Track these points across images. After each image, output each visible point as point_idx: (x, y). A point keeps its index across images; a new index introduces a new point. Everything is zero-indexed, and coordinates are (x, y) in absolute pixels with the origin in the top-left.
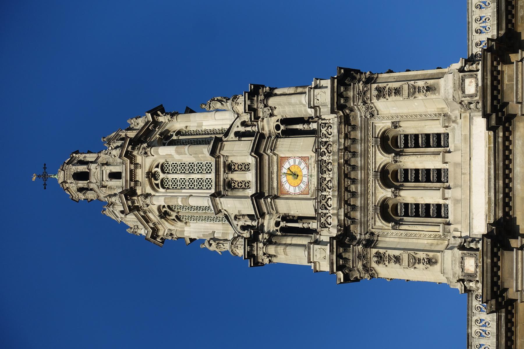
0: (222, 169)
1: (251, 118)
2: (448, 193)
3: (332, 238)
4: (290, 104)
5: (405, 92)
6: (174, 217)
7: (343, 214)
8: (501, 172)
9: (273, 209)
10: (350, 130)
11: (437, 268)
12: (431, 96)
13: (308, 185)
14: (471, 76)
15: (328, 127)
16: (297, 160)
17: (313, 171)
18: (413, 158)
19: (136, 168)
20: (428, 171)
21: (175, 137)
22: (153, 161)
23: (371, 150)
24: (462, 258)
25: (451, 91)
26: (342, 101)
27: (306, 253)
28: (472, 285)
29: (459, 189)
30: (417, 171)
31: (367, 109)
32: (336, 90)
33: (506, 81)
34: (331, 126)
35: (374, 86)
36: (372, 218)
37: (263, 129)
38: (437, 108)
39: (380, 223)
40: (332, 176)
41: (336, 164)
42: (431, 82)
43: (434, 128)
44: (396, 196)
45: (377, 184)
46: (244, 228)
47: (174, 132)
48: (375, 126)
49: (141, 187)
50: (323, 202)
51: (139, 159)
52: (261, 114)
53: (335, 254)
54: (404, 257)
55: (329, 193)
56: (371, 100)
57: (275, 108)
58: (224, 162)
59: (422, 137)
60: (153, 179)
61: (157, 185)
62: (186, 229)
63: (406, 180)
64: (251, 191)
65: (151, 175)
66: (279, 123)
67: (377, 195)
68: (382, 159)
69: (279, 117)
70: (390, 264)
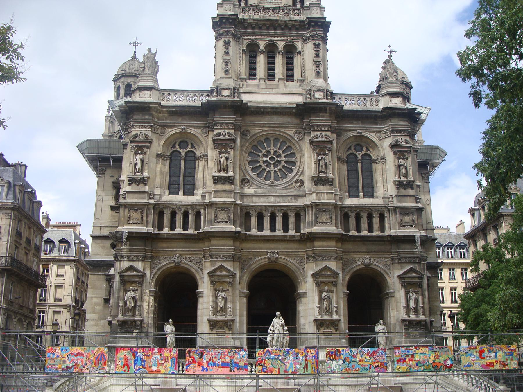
3: (237, 15)
5: (317, 60)
8: (274, 110)
11: (224, 75)
12: (314, 73)
18: (281, 62)
20: (274, 70)
23: (285, 39)
24: (229, 89)
25: (317, 85)
26: (313, 24)
28: (215, 94)
29: (265, 87)
30: (274, 64)
31: (308, 38)
33: (321, 114)
35: (321, 42)
39: (246, 42)
40: (271, 16)
41: (278, 19)
42: (322, 74)
43: (297, 75)
44: (260, 52)
50: (256, 10)
63: (269, 57)
68: (281, 45)
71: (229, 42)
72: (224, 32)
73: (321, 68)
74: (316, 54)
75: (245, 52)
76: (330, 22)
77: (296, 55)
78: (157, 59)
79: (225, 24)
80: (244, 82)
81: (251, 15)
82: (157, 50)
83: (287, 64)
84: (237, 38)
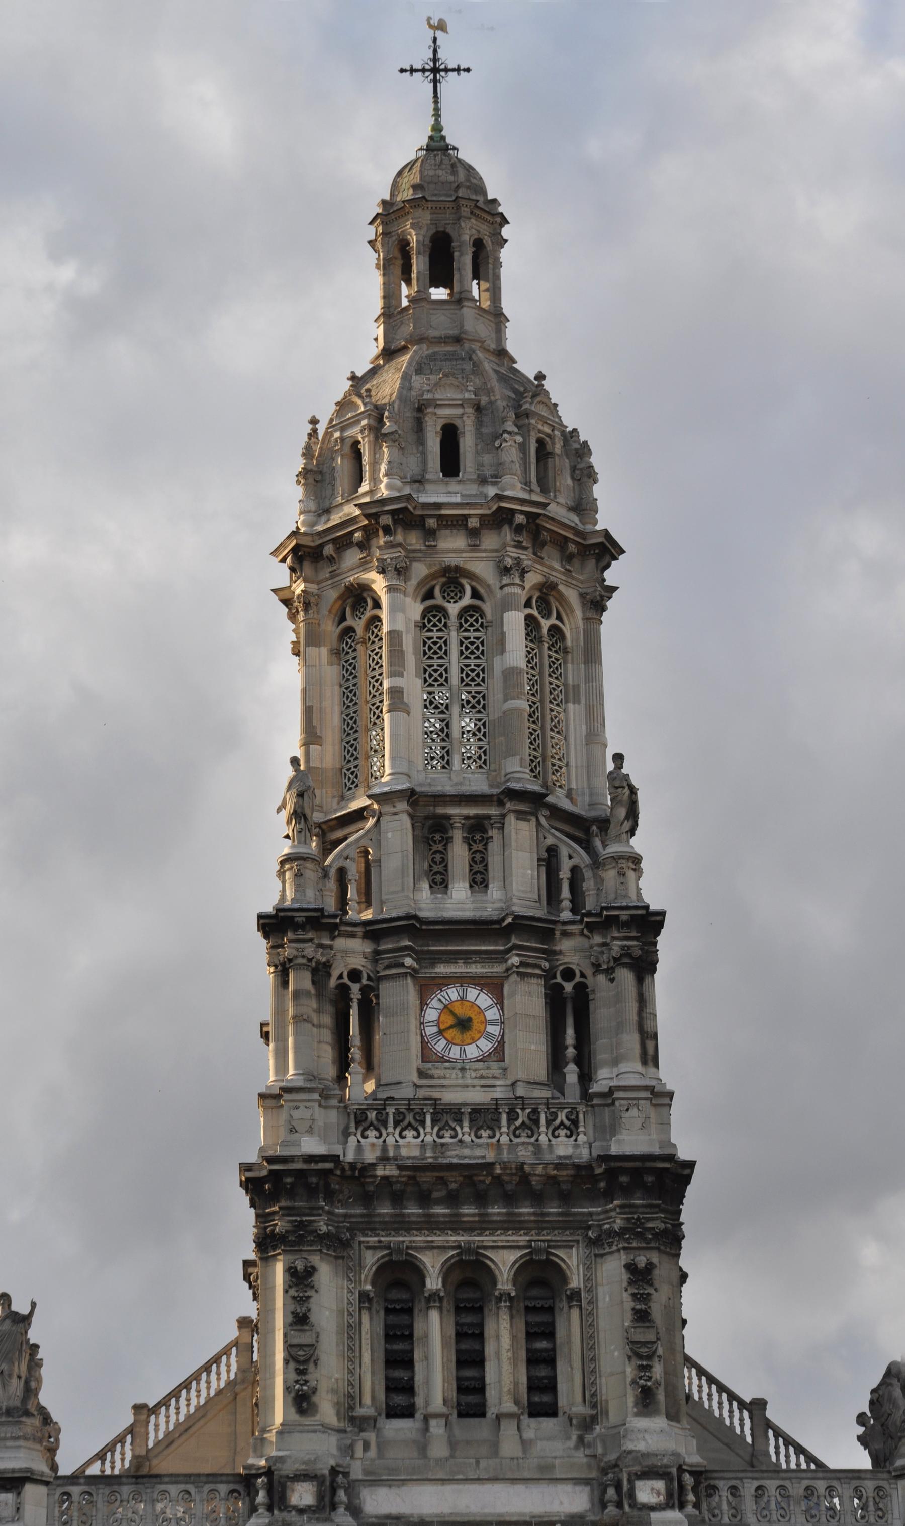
0: (472, 811)
1: (589, 914)
2: (438, 1426)
4: (620, 1028)
6: (350, 622)
7: (387, 1173)
9: (388, 967)
10: (564, 1187)
11: (294, 1416)
13: (443, 1060)
14: (669, 1494)
15: (568, 1128)
16: (494, 1030)
17: (473, 1075)
18: (506, 1341)
19: (474, 533)
21: (545, 624)
22: (489, 586)
23: (522, 1239)
25: (641, 1446)
26: (624, 1179)
27: (300, 1082)
28: (261, 1497)
32: (649, 1164)
34: (570, 1136)
35: (655, 1258)
36: (380, 1242)
37: (565, 934)
38: (607, 1401)
39: (371, 1259)
41: (491, 1157)
42: (661, 1396)
45: (452, 1253)
46: (342, 872)
47: (559, 617)
48: (571, 1247)
49: (423, 548)
51: (490, 541)
52: (598, 939)
53: (305, 1167)
54: (308, 1333)
55: (429, 1134)
56: (625, 1248)
57: (612, 980)
58: (489, 817)
59: (546, 1350)
60: (444, 579)
61: (429, 595)
62: (324, 651)
64: (426, 903)
65: (453, 579)
66: (578, 979)
67: (428, 1253)
68: (505, 1263)
69: (590, 981)
70: (290, 1301)
71: (311, 1271)
72: (288, 1226)
73: (658, 1370)
74: (636, 1311)
75: (370, 1300)
76: (691, 1165)
77: (564, 1304)
78: (33, 1336)
79: (291, 1194)
80: (371, 1436)
81: (390, 1140)
82: (34, 1305)
83: (531, 1336)
84: (338, 1245)
